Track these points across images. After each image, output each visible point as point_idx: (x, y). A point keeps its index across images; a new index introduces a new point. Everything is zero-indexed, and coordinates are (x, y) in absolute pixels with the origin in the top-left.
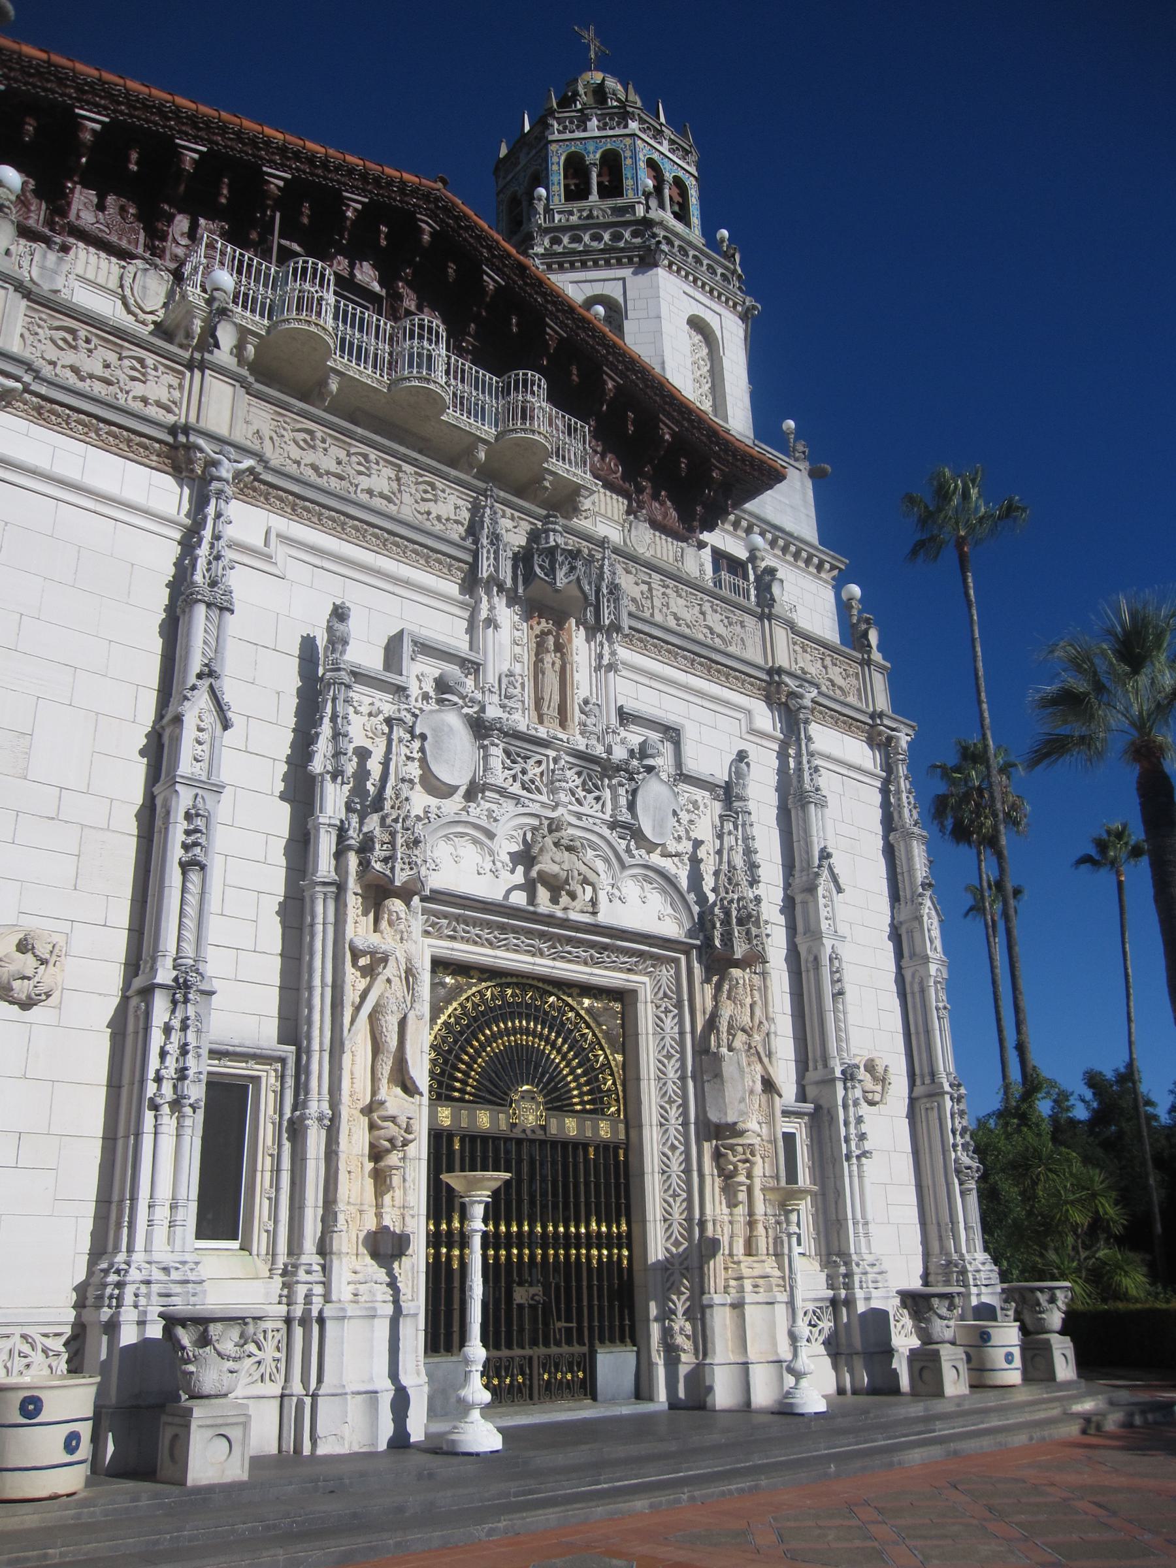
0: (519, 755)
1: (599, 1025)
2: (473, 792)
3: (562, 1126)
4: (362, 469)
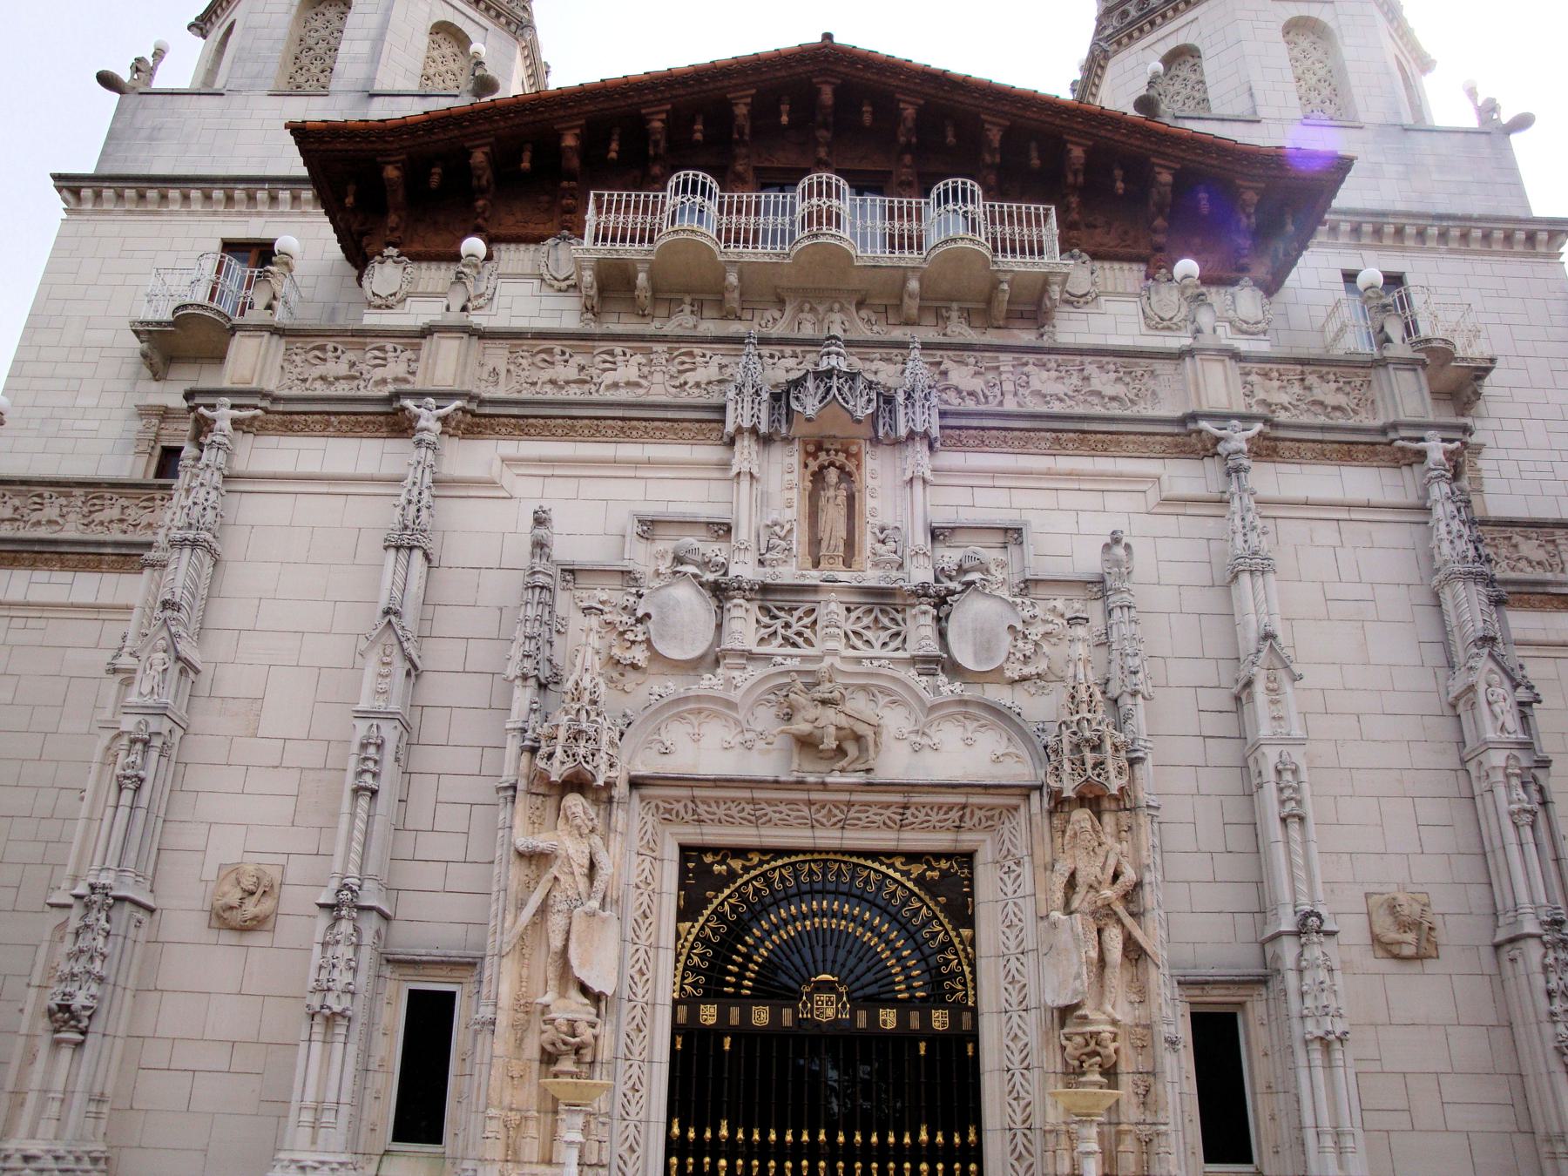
0: (780, 609)
1: (934, 897)
2: (714, 659)
3: (873, 1019)
4: (608, 365)
